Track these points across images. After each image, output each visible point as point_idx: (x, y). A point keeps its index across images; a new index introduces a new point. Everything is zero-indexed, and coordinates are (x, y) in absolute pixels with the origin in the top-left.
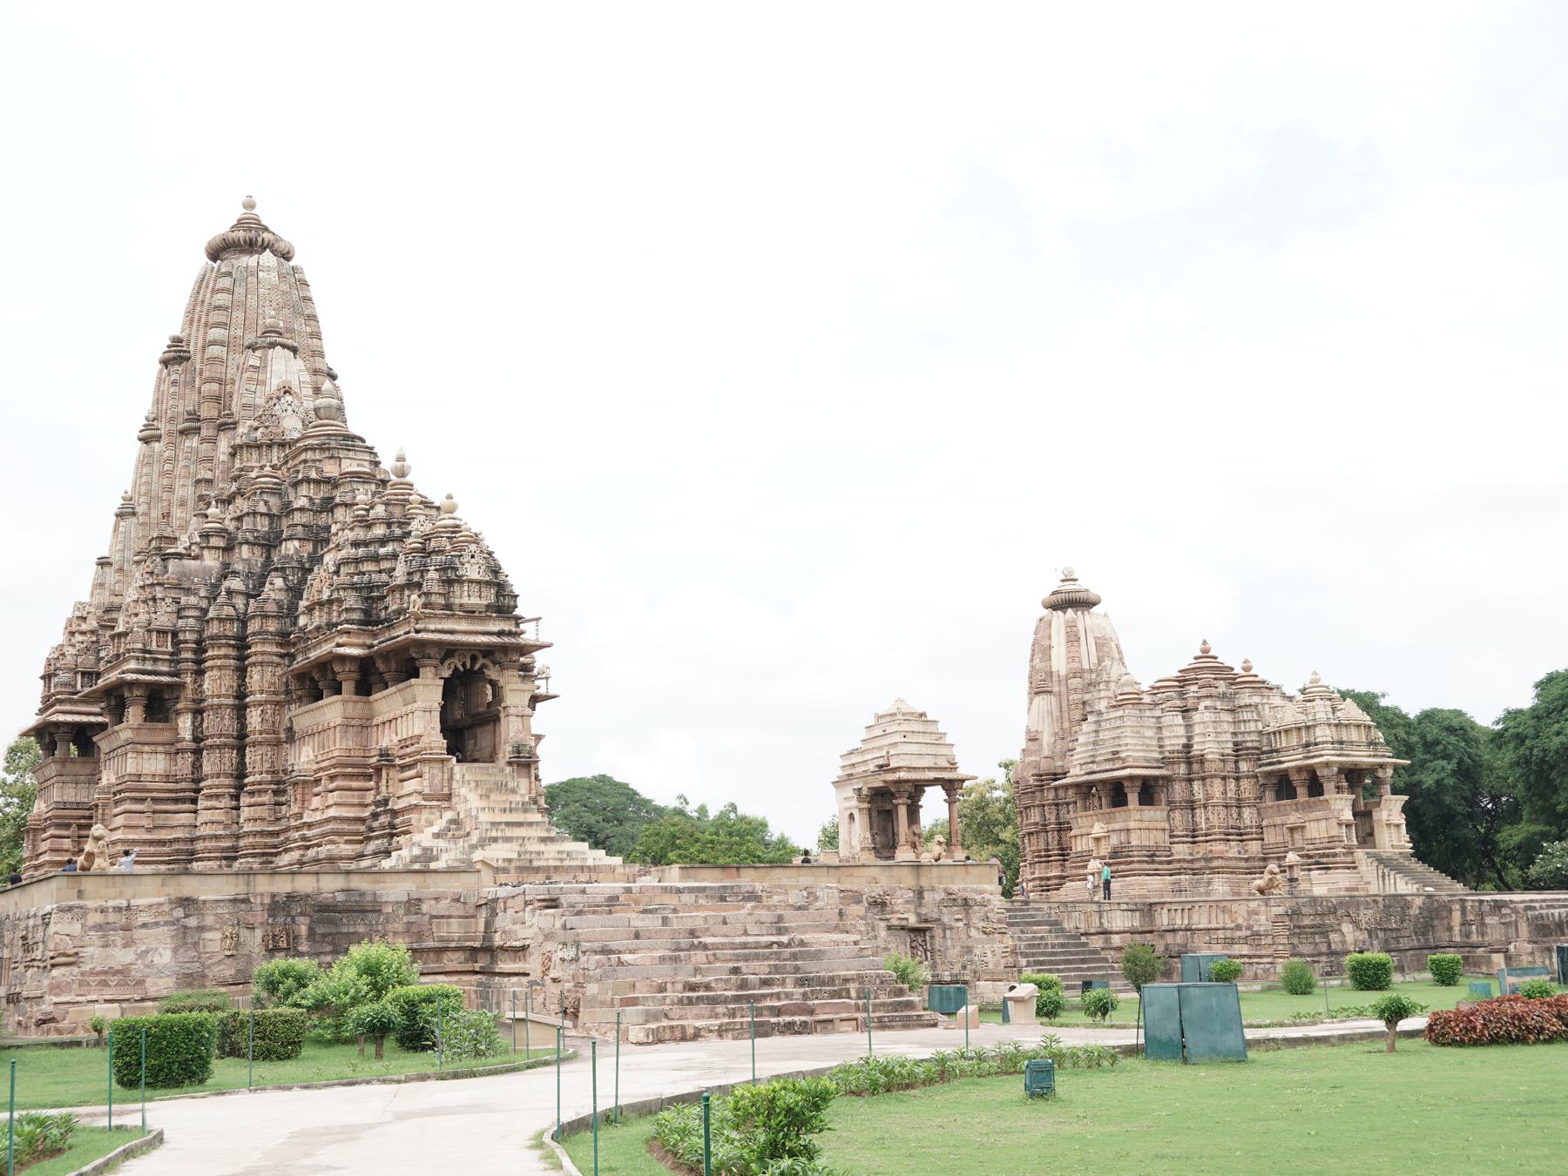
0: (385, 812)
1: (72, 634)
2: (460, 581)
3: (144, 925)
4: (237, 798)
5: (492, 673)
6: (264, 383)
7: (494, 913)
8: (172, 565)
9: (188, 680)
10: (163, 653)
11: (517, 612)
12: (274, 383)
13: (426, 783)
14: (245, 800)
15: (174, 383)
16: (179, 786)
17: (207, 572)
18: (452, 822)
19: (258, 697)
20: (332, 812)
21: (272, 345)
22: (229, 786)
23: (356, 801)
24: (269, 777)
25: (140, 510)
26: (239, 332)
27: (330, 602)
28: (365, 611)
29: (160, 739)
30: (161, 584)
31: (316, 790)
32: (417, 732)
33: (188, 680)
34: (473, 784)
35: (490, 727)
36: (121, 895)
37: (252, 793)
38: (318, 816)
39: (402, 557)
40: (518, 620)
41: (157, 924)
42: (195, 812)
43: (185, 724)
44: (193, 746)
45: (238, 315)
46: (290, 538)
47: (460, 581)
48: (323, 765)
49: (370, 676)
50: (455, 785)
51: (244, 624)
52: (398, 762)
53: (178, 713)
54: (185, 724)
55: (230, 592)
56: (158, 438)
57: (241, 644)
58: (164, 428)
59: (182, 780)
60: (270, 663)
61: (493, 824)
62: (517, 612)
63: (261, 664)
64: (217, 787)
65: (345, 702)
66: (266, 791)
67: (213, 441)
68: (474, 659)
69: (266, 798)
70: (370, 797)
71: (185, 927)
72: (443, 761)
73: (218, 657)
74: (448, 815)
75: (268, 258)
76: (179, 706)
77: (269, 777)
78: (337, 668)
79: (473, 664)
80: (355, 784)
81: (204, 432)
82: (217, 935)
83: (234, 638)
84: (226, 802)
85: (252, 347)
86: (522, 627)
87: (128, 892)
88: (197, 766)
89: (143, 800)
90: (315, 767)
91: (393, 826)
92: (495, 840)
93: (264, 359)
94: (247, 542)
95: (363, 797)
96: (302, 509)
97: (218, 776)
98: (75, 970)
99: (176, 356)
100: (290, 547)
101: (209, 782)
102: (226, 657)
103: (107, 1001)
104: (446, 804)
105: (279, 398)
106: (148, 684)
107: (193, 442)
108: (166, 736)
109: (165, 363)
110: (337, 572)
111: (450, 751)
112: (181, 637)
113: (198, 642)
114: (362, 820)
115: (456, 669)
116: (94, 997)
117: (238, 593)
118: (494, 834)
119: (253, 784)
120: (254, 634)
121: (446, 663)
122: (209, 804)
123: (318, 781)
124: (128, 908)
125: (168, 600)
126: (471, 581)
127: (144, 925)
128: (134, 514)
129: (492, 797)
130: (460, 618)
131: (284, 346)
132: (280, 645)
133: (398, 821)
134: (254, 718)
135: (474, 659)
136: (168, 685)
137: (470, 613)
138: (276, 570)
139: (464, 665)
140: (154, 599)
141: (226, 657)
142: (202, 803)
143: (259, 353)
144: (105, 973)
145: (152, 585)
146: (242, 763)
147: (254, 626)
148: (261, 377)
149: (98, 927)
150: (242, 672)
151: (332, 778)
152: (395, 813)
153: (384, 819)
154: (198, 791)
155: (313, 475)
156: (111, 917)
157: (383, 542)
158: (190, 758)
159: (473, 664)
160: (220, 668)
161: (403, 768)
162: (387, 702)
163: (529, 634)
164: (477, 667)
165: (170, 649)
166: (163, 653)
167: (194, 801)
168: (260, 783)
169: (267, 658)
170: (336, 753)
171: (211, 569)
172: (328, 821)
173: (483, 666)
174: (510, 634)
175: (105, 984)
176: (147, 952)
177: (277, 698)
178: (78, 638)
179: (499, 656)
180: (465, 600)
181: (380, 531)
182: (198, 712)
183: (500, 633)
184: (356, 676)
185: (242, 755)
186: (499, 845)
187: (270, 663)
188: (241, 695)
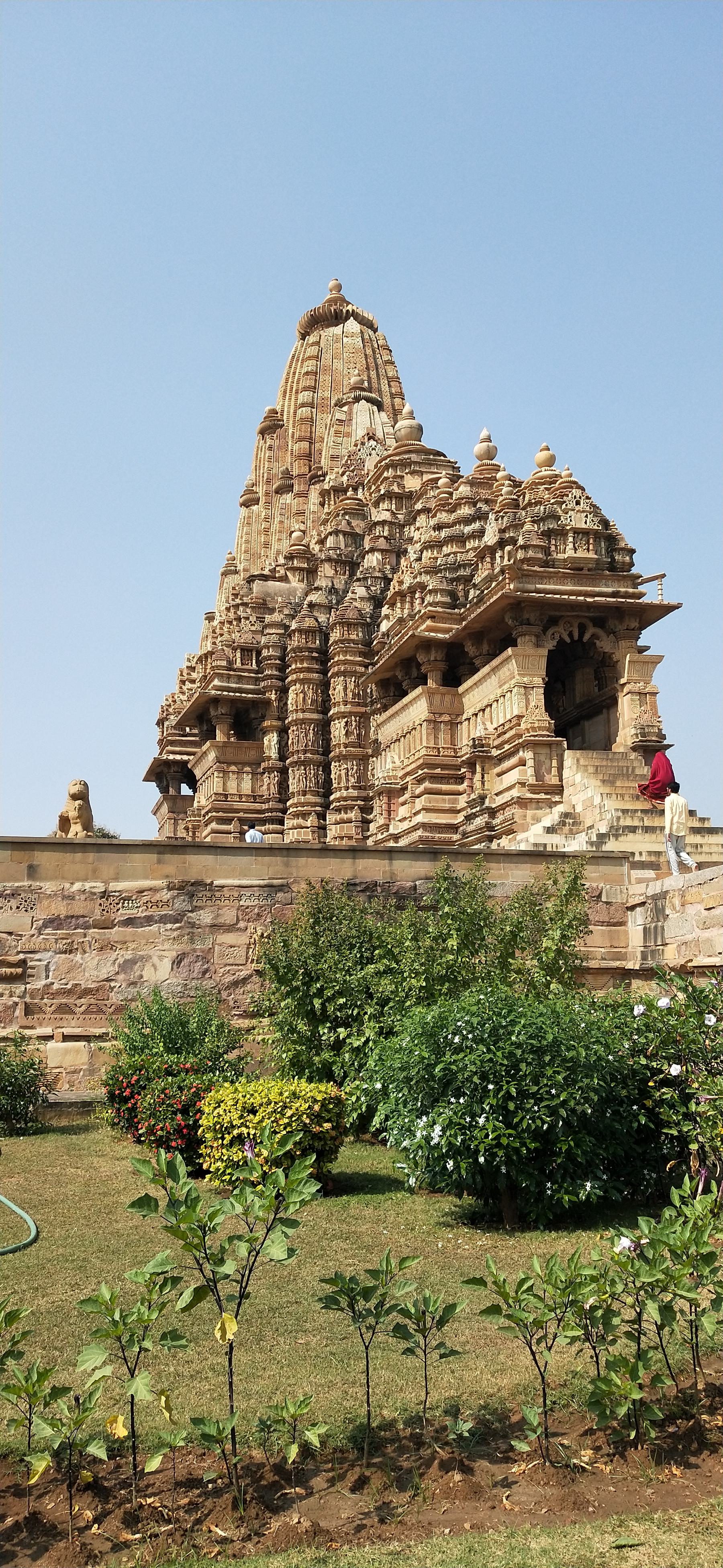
0: (482, 812)
1: (183, 682)
2: (562, 533)
3: (130, 922)
4: (322, 816)
5: (605, 644)
6: (349, 435)
7: (659, 913)
8: (257, 586)
9: (273, 697)
10: (249, 671)
11: (634, 571)
12: (359, 431)
13: (530, 771)
14: (331, 818)
15: (270, 448)
16: (265, 806)
17: (292, 592)
18: (566, 815)
19: (342, 708)
20: (420, 818)
21: (357, 399)
22: (315, 805)
23: (447, 806)
24: (355, 793)
25: (240, 567)
26: (327, 394)
27: (412, 590)
28: (453, 594)
29: (246, 759)
30: (245, 605)
31: (402, 799)
32: (516, 713)
33: (273, 697)
34: (591, 770)
35: (601, 718)
36: (94, 875)
37: (338, 810)
38: (406, 825)
39: (492, 516)
40: (635, 580)
41: (149, 920)
42: (282, 832)
43: (271, 741)
44: (280, 764)
45: (325, 379)
46: (372, 550)
47: (562, 533)
48: (409, 769)
49: (456, 664)
50: (566, 773)
51: (326, 637)
52: (495, 753)
53: (265, 732)
54: (271, 741)
55: (311, 605)
56: (257, 501)
57: (323, 657)
58: (261, 490)
59: (268, 800)
60: (353, 673)
61: (625, 812)
62: (634, 571)
63: (344, 674)
64: (303, 805)
65: (430, 694)
66: (352, 808)
67: (304, 495)
68: (582, 629)
69: (352, 815)
70: (462, 802)
71: (193, 925)
72: (549, 745)
73: (301, 670)
74: (560, 809)
75: (352, 325)
76: (267, 723)
77: (355, 793)
78: (421, 658)
79: (581, 635)
80: (444, 787)
81: (296, 488)
82: (241, 939)
83: (316, 650)
84: (311, 821)
85: (340, 404)
86: (641, 589)
87: (107, 870)
88: (283, 785)
89: (228, 821)
90: (400, 773)
91: (490, 828)
92: (633, 829)
93: (350, 413)
94: (329, 560)
95: (456, 801)
96: (383, 523)
97: (304, 793)
98: (20, 988)
99: (272, 426)
100: (372, 560)
101: (295, 800)
103: (66, 1038)
104: (557, 798)
105: (363, 444)
106: (233, 701)
107: (288, 498)
108: (252, 755)
109: (263, 432)
110: (419, 559)
111: (559, 731)
112: (265, 653)
113: (282, 658)
114: (454, 828)
115: (561, 642)
116: (47, 1031)
117: (320, 605)
118: (628, 822)
119: (338, 800)
120: (336, 642)
121: (550, 632)
122: (295, 822)
123: (404, 789)
124: (105, 895)
125: (253, 619)
126: (577, 532)
127: (130, 922)
128: (236, 572)
129: (618, 783)
130: (565, 576)
131: (368, 400)
132: (362, 654)
133: (495, 822)
134: (338, 730)
135: (582, 629)
136: (254, 702)
138: (359, 580)
139: (571, 635)
140: (239, 619)
141: (309, 670)
142: (289, 823)
143: (345, 409)
144: (69, 992)
145: (236, 606)
146: (328, 782)
147: (335, 636)
148: (347, 429)
149: (54, 922)
150: (325, 686)
151: (420, 781)
152: (493, 813)
153: (479, 821)
154: (284, 811)
155: (395, 488)
156: (79, 907)
157: (468, 521)
158: (275, 777)
159: (581, 635)
160: (302, 681)
161: (501, 759)
162: (477, 692)
163: (651, 595)
164: (586, 637)
165: (254, 666)
166: (249, 671)
167: (281, 822)
168: (345, 799)
169: (349, 668)
170: (423, 752)
171: (295, 590)
172: (415, 828)
173: (594, 636)
174: (627, 595)
175: (65, 1010)
176: (132, 962)
177: (363, 709)
178: (188, 685)
179: (612, 623)
181: (466, 511)
182: (283, 732)
183: (615, 595)
184: (442, 666)
185: (327, 770)
186: (639, 836)
187: (353, 673)
188: (325, 705)
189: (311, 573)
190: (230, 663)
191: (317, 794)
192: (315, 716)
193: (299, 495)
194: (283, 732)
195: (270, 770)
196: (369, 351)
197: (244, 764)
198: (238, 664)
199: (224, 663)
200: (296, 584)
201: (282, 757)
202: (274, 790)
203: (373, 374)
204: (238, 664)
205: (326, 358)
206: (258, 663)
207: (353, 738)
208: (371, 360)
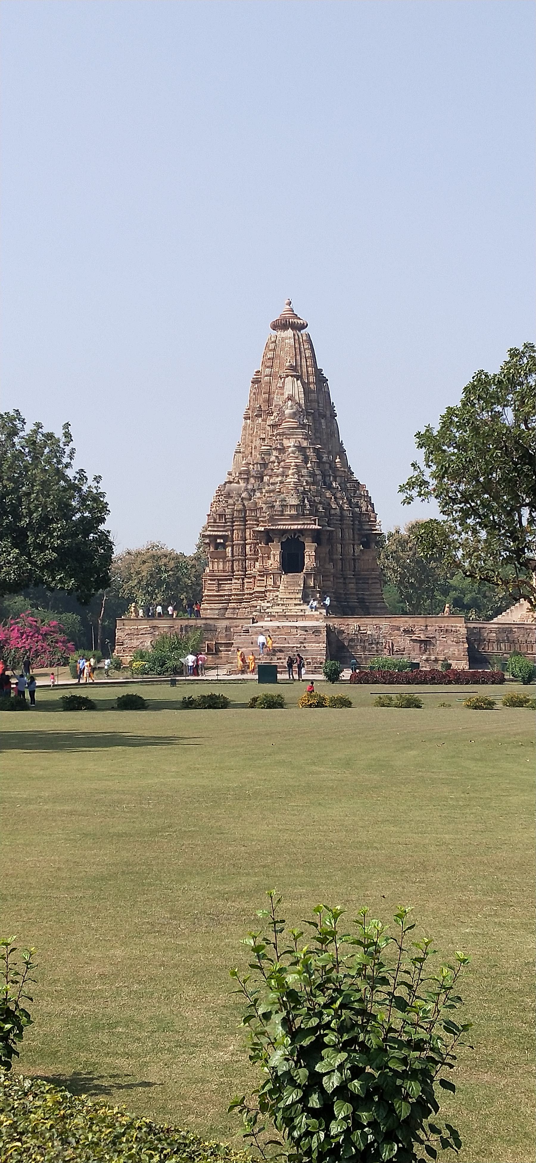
14: (246, 580)
16: (227, 574)
21: (287, 376)
45: (277, 361)
53: (227, 546)
83: (242, 517)
89: (214, 580)
102: (240, 525)
108: (223, 555)
126: (290, 505)
137: (292, 517)
140: (219, 501)
141: (240, 525)
177: (256, 541)
180: (289, 513)
182: (232, 546)
189: (247, 480)
190: (215, 520)
191: (242, 571)
192: (242, 542)
193: (263, 420)
194: (232, 546)
195: (229, 561)
196: (297, 346)
197: (220, 558)
198: (218, 521)
199: (212, 521)
200: (242, 484)
201: (233, 556)
202: (230, 568)
203: (298, 357)
204: (218, 521)
205: (278, 352)
206: (225, 519)
207: (253, 552)
208: (298, 350)
